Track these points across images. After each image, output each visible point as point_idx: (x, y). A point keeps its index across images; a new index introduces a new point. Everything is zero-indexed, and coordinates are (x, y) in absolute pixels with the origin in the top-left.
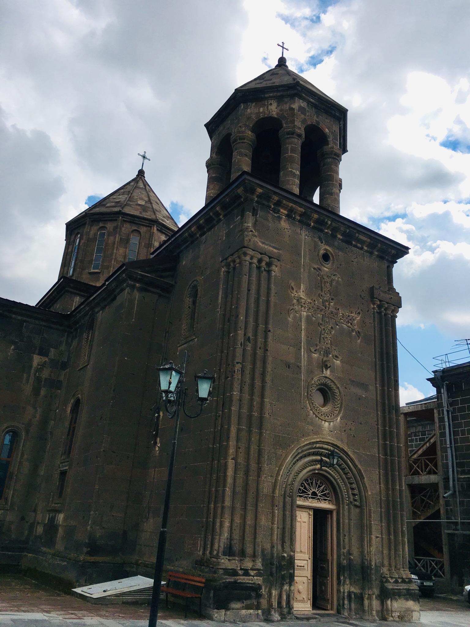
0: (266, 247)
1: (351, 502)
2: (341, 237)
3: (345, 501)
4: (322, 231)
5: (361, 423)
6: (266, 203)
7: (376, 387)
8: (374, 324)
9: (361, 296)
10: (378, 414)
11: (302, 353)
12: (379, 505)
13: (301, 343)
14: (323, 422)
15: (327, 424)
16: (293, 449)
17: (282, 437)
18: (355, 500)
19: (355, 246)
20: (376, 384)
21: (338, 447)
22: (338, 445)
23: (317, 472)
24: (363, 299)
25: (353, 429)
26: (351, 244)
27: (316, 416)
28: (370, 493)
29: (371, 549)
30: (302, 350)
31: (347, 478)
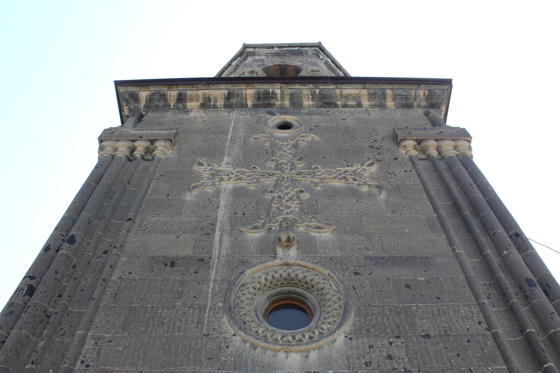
0: (145, 132)
2: (311, 103)
4: (270, 105)
5: (427, 336)
6: (160, 104)
7: (457, 256)
8: (417, 170)
9: (372, 147)
10: (482, 308)
11: (217, 238)
13: (213, 225)
19: (345, 106)
20: (454, 250)
24: (378, 149)
26: (336, 106)
30: (218, 233)
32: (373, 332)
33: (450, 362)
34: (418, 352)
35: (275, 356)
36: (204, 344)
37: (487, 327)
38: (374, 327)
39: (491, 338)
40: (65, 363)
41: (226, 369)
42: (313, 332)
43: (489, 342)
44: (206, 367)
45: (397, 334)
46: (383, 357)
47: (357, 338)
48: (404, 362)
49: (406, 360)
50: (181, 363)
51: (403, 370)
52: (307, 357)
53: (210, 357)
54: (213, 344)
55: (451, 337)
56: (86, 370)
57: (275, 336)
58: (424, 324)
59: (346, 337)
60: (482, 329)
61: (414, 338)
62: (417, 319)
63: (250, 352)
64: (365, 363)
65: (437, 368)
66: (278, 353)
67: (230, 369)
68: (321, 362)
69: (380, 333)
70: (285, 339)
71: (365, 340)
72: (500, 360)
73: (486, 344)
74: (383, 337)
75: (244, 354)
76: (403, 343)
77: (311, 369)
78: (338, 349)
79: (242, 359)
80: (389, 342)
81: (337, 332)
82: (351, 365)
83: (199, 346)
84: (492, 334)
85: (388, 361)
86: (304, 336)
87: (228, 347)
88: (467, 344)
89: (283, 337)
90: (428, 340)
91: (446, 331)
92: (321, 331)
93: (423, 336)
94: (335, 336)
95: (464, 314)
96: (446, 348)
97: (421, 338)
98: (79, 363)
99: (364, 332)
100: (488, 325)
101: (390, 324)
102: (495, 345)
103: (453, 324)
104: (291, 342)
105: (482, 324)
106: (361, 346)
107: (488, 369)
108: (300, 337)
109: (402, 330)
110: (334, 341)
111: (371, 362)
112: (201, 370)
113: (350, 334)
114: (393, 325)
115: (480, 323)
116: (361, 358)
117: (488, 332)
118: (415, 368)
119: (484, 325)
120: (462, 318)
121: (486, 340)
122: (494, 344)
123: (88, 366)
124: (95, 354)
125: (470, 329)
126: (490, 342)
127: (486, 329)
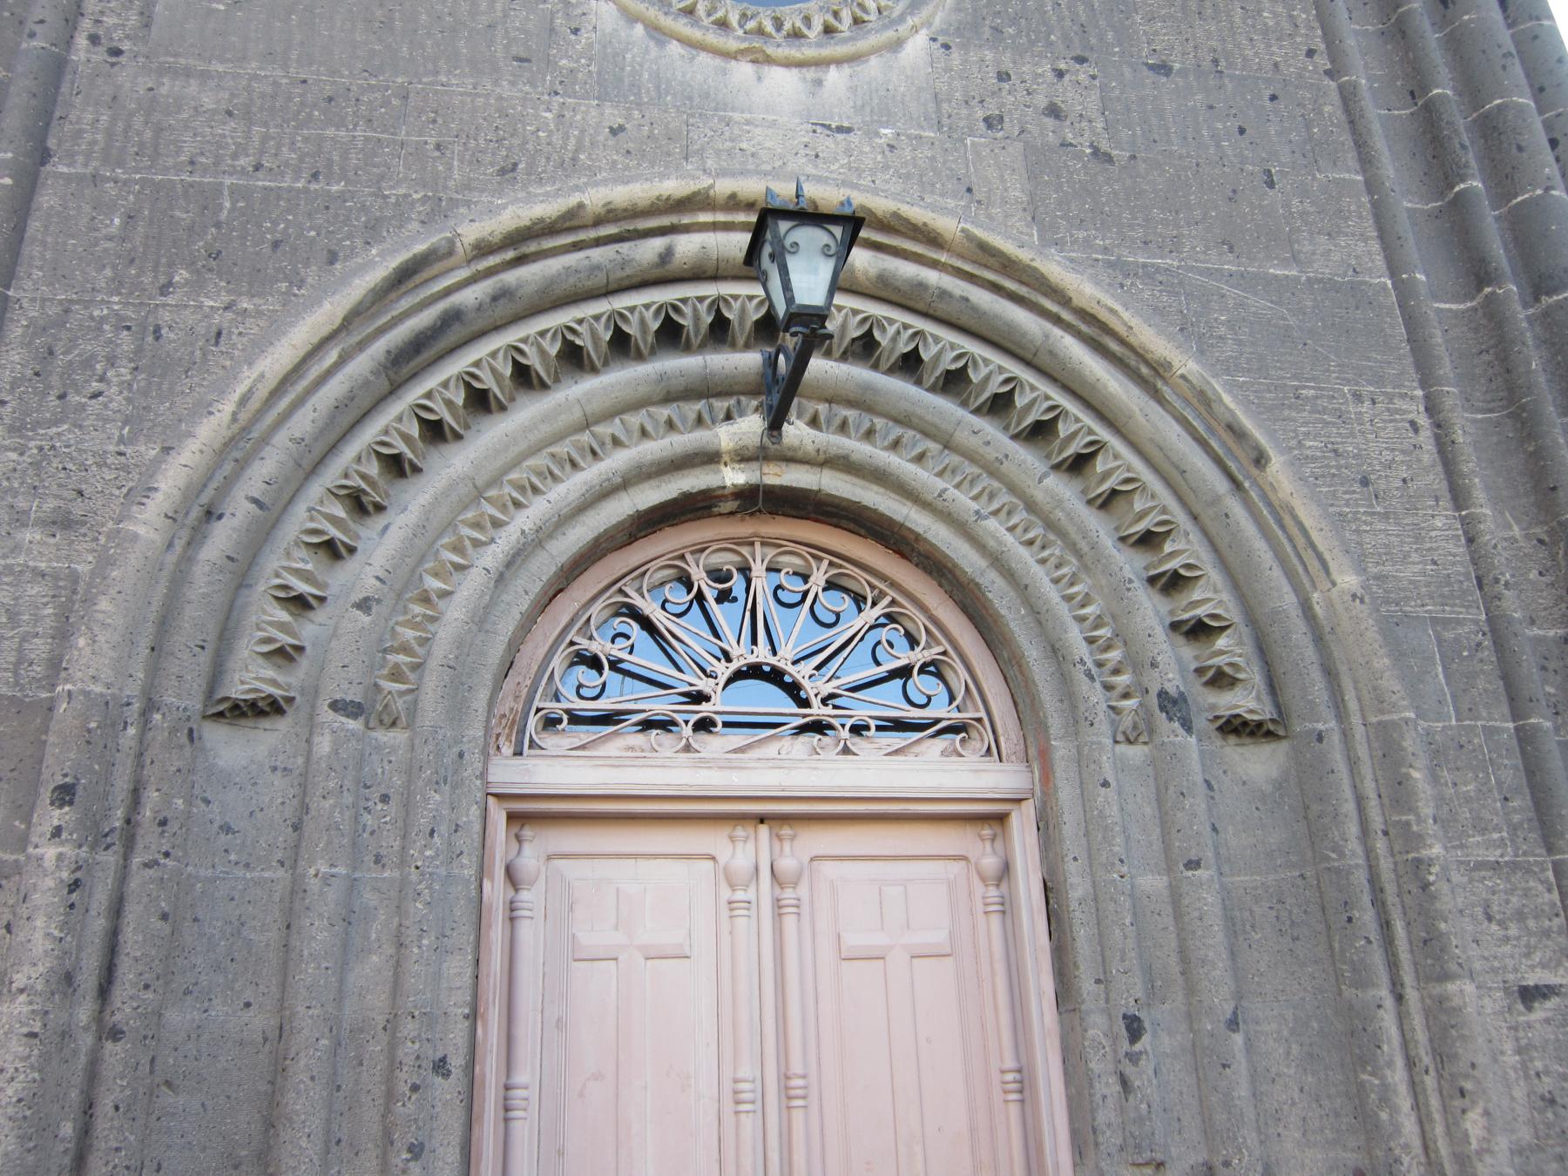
1: (1171, 704)
3: (1094, 695)
5: (1163, 69)
12: (1487, 682)
14: (743, 70)
15: (783, 84)
16: (369, 265)
17: (234, 190)
18: (1221, 680)
21: (932, 239)
22: (917, 213)
23: (734, 476)
25: (1079, 97)
27: (657, 33)
28: (1348, 580)
29: (1474, 1124)
31: (1107, 501)
32: (1011, 37)
33: (1218, 146)
34: (1134, 107)
35: (724, 72)
36: (499, 14)
37: (1329, 66)
38: (1014, 21)
39: (1335, 97)
40: (32, 35)
41: (574, 95)
42: (836, 14)
43: (1327, 109)
44: (513, 83)
45: (1078, 52)
46: (1036, 108)
47: (964, 46)
48: (1093, 130)
49: (1099, 125)
50: (430, 66)
51: (1088, 151)
52: (819, 83)
53: (523, 55)
54: (527, 18)
55: (1226, 81)
56: (113, 65)
57: (719, 14)
58: (1156, 33)
59: (934, 40)
60: (1315, 71)
61: (1127, 71)
62: (1138, 19)
63: (647, 51)
64: (986, 120)
65: (1181, 157)
66: (733, 63)
67: (586, 96)
68: (859, 103)
69: (1032, 43)
70: (751, 25)
71: (989, 55)
72: (1351, 158)
73: (1321, 113)
74: (1040, 55)
75: (629, 56)
76: (1093, 77)
77: (832, 118)
78: (909, 73)
79: (623, 69)
80: (1054, 70)
81: (910, 21)
82: (945, 121)
83: (484, 20)
84: (1341, 88)
85: (1050, 122)
86: (807, 20)
87: (576, 31)
88: (1268, 103)
89: (744, 17)
90: (1164, 79)
91: (1215, 62)
92: (859, 13)
93: (1151, 67)
94: (903, 29)
95: (1271, 23)
96: (1211, 107)
97: (1146, 72)
98: (81, 41)
99: (987, 33)
100: (1332, 62)
101: (1061, 19)
102: (1343, 117)
103: (1238, 45)
104: (770, 36)
105: (1317, 58)
106: (975, 70)
107: (1314, 178)
108: (799, 24)
109: (1093, 41)
110: (897, 45)
111: (1001, 119)
112: (498, 90)
113: (943, 32)
114: (1068, 23)
115: (1310, 53)
116: (974, 103)
117: (1326, 81)
118: (1123, 150)
119: (1323, 62)
120: (1266, 32)
121: (1321, 101)
122: (1340, 115)
123: (117, 52)
124: (134, 19)
125: (1282, 66)
126: (1332, 108)
127: (1327, 72)
